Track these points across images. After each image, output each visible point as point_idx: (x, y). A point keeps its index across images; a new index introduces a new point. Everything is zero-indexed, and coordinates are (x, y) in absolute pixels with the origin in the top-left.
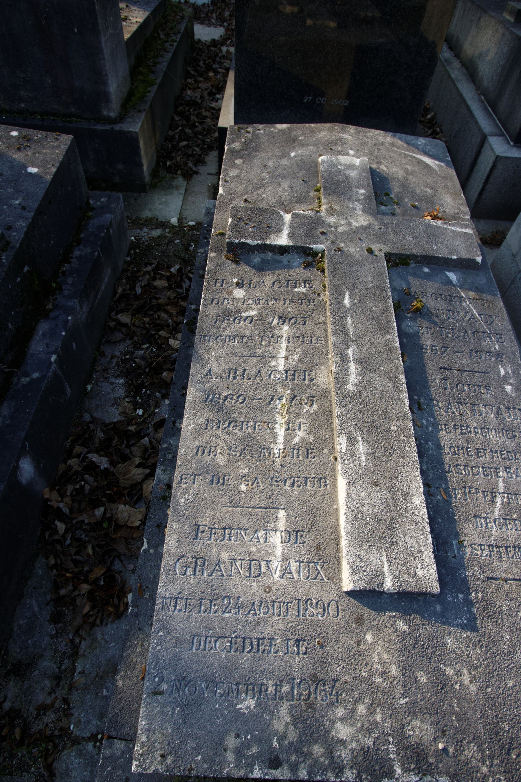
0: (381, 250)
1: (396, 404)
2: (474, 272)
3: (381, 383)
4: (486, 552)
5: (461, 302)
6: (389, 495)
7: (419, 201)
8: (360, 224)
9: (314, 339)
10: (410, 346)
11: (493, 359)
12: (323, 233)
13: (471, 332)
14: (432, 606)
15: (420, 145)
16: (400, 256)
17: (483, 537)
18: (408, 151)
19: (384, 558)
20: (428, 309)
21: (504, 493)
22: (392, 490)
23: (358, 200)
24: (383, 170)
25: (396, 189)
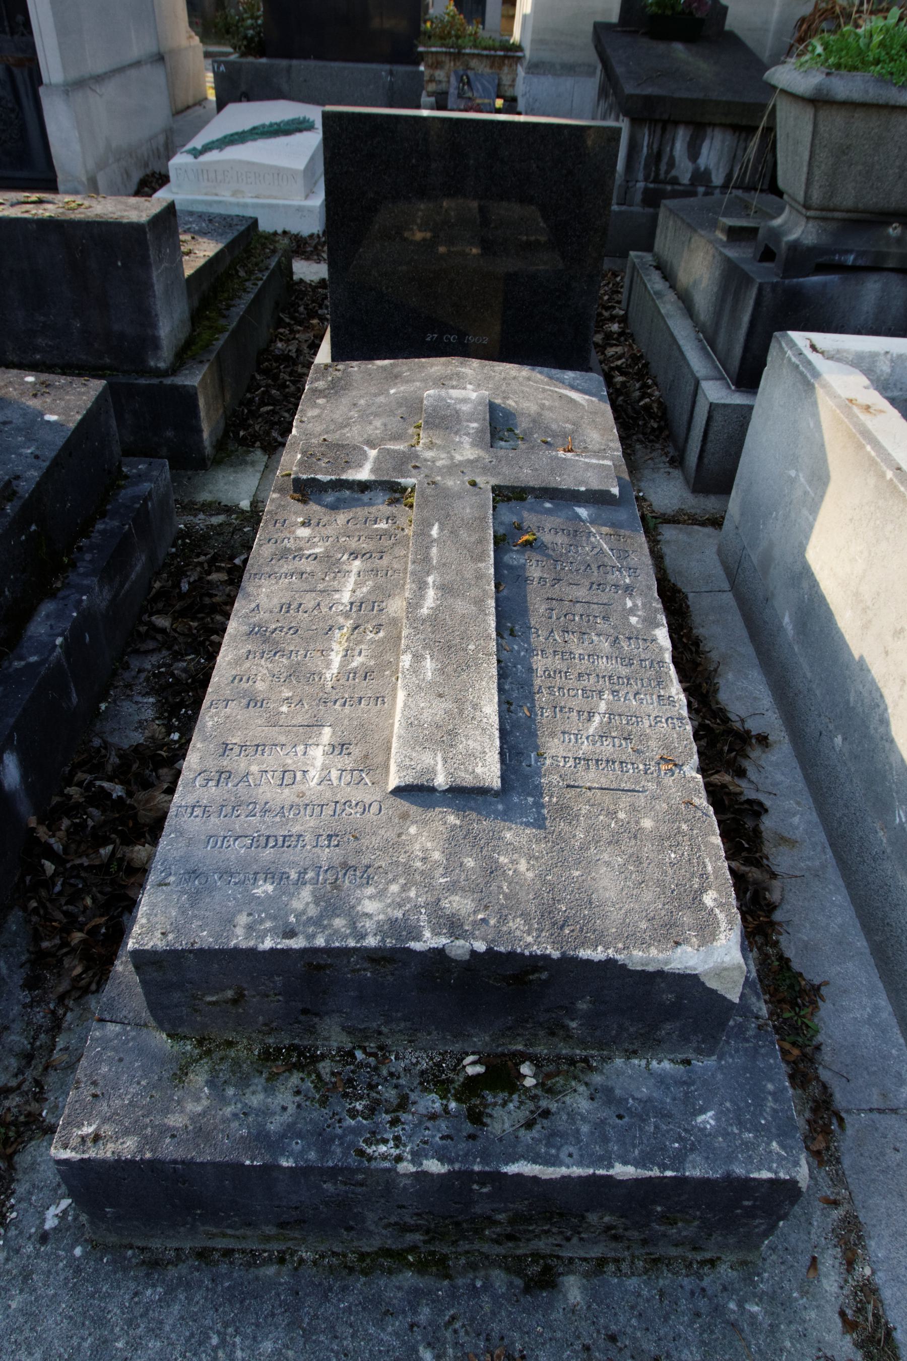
12: (415, 467)
16: (512, 489)
22: (459, 702)
23: (468, 434)
25: (523, 424)
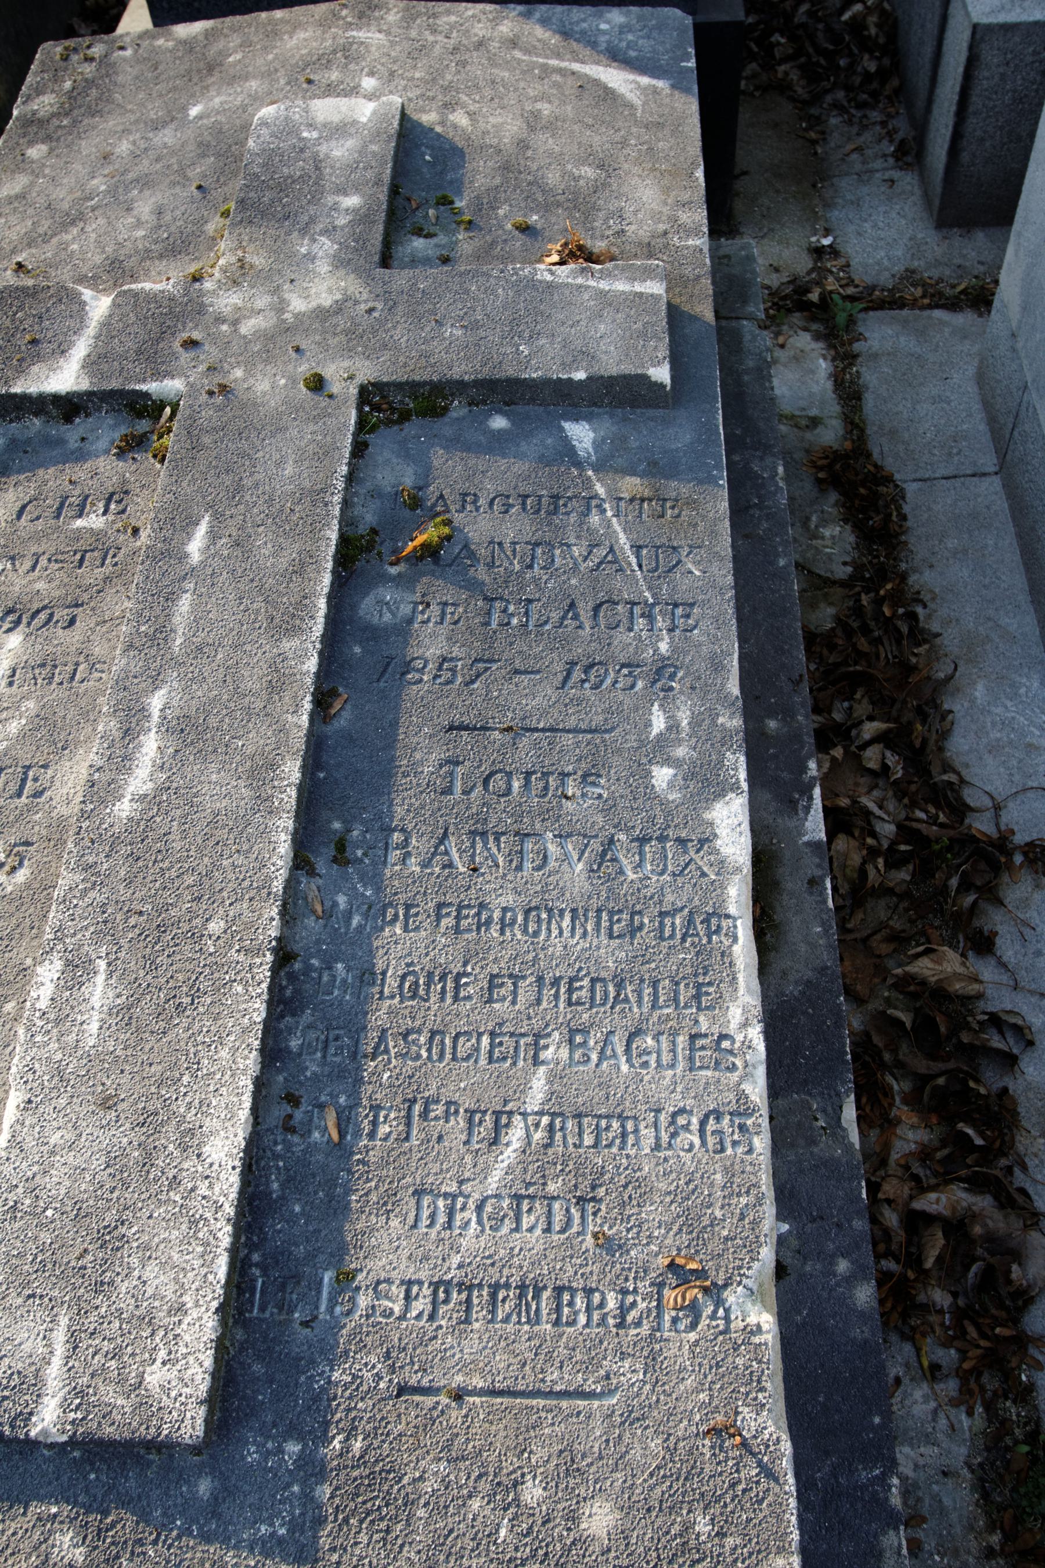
0: (351, 378)
1: (248, 851)
2: (659, 413)
3: (219, 788)
4: (420, 1305)
5: (586, 513)
6: (137, 1136)
7: (546, 208)
8: (314, 304)
9: (81, 668)
10: (356, 669)
11: (640, 684)
12: (191, 344)
13: (591, 605)
14: (187, 1482)
15: (604, 32)
16: (411, 388)
17: (426, 1258)
18: (559, 56)
19: (60, 1336)
20: (466, 546)
21: (541, 1113)
22: (148, 1121)
23: (330, 231)
24: (455, 127)
25: (480, 176)
